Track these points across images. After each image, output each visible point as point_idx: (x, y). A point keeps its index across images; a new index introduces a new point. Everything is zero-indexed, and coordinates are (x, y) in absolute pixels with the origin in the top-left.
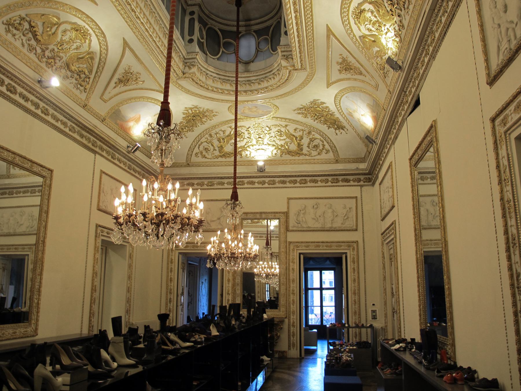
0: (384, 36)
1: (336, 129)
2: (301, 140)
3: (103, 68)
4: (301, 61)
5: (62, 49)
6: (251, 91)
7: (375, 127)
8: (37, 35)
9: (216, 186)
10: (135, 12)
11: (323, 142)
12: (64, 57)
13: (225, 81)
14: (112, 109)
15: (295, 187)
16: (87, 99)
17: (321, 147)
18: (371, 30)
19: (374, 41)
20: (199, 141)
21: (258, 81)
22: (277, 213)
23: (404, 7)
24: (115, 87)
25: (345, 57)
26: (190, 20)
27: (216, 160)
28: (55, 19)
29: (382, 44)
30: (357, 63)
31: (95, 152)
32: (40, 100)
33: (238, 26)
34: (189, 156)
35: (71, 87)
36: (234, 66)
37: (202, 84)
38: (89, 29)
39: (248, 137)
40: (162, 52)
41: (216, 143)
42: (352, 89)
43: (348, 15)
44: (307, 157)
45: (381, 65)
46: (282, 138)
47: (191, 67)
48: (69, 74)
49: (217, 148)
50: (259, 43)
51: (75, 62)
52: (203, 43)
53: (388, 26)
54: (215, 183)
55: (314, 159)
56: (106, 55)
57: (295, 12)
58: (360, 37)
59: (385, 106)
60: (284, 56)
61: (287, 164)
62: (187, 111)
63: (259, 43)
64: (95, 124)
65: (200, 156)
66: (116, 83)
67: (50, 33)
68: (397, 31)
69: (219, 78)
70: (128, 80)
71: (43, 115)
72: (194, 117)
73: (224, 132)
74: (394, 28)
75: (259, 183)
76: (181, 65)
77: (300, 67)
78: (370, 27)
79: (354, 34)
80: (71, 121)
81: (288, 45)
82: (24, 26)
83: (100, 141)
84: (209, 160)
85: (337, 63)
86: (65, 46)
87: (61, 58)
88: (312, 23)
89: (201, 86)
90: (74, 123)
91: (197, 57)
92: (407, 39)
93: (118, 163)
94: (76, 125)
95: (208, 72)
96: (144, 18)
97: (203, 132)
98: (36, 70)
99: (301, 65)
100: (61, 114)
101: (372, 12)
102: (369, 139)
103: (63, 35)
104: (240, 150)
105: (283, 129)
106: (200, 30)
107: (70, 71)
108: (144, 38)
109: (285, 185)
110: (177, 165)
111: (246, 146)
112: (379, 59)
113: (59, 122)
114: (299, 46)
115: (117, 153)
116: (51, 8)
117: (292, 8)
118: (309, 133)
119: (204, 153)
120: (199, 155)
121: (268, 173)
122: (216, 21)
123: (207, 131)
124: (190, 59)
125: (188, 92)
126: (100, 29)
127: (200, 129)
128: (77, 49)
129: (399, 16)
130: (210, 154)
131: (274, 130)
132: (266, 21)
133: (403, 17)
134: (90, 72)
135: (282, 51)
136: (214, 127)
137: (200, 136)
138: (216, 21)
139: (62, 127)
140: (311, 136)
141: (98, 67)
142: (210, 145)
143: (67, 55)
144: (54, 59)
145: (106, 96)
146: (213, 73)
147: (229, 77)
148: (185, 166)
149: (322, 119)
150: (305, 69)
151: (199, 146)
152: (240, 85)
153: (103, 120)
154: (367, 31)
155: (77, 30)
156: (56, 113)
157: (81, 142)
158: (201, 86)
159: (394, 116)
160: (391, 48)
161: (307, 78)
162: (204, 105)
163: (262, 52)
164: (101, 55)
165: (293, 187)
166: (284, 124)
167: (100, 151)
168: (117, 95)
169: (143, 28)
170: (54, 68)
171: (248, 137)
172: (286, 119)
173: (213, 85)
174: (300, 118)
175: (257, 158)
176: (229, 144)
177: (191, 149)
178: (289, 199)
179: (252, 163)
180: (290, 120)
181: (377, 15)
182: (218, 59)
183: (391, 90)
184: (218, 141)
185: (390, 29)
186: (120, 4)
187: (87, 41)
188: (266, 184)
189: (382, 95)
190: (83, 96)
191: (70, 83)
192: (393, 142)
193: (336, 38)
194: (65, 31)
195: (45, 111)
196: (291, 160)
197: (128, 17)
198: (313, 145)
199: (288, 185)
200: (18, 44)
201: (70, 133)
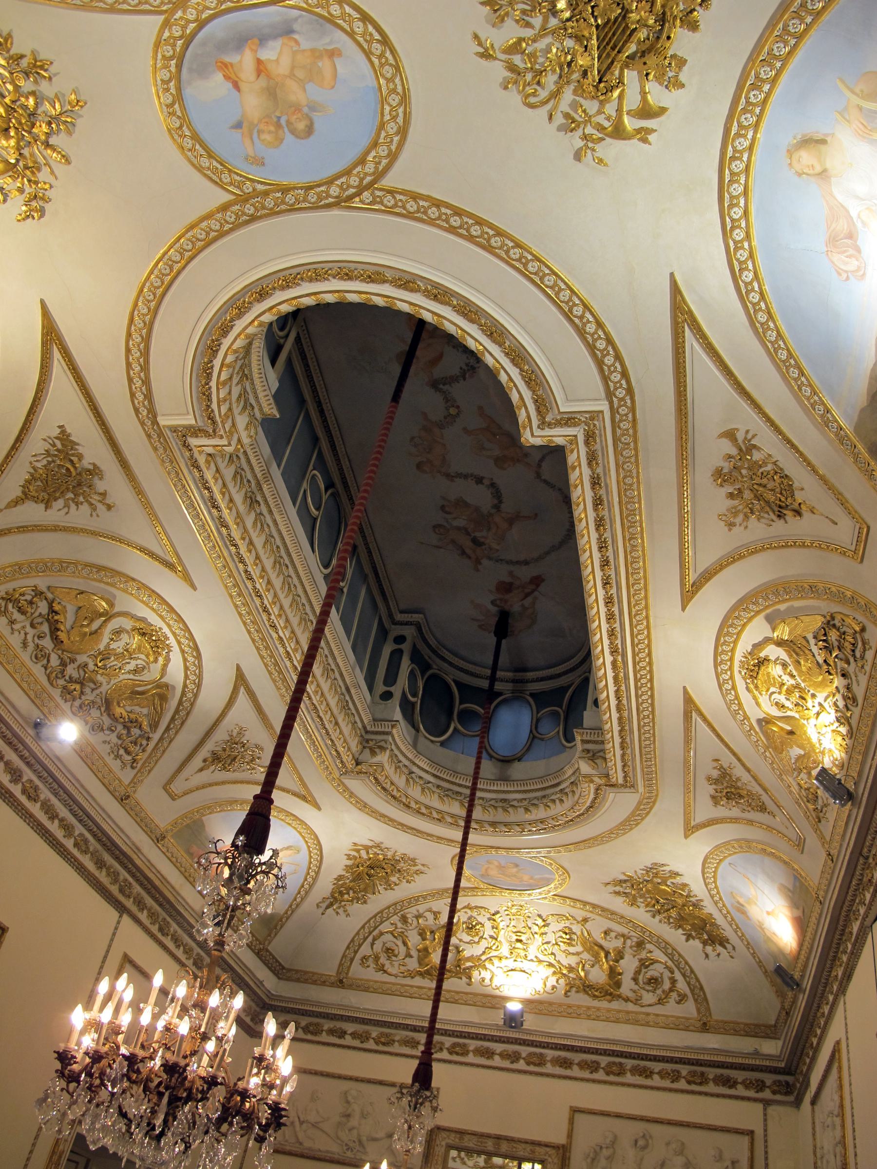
0: (813, 721)
1: (705, 943)
2: (617, 961)
3: (182, 724)
4: (624, 766)
5: (105, 667)
6: (506, 824)
7: (801, 945)
8: (58, 630)
9: (396, 1048)
10: (269, 614)
11: (672, 972)
12: (105, 683)
13: (450, 793)
14: (185, 816)
15: (594, 1081)
16: (134, 783)
17: (667, 985)
18: (783, 706)
19: (791, 733)
20: (376, 928)
21: (525, 803)
22: (539, 1144)
23: (854, 656)
24: (201, 770)
25: (725, 766)
26: (393, 653)
27: (408, 981)
28: (104, 604)
29: (809, 739)
30: (754, 783)
31: (121, 909)
32: (28, 764)
33: (493, 679)
34: (347, 959)
35: (104, 750)
36: (473, 760)
37: (395, 793)
38: (170, 635)
39: (492, 937)
40: (316, 708)
41: (414, 939)
42: (745, 846)
43: (731, 668)
44: (631, 1007)
45: (808, 789)
46: (572, 949)
47: (377, 750)
48: (107, 721)
49: (414, 953)
50: (538, 720)
51: (126, 699)
52: (413, 705)
53: (820, 697)
54: (397, 1038)
55: (648, 1014)
56: (196, 696)
57: (612, 653)
58: (759, 721)
59: (821, 893)
60: (588, 751)
61: (578, 1016)
62: (358, 851)
63: (538, 720)
64: (138, 844)
65: (373, 965)
66: (205, 761)
67: (87, 630)
68: (840, 711)
69: (438, 787)
70: (235, 758)
71: (23, 799)
72: (370, 871)
74: (835, 704)
75: (504, 1055)
76: (354, 744)
77: (621, 781)
78: (782, 698)
79: (744, 712)
80: (84, 826)
81: (599, 729)
82: (37, 607)
83: (141, 885)
84: (392, 979)
85: (709, 779)
86: (112, 662)
87: (97, 685)
88: (651, 680)
89: (393, 796)
90: (90, 831)
91: (394, 731)
92: (866, 730)
93: (171, 945)
94: (94, 836)
95: (415, 769)
96: (286, 627)
97: (388, 907)
98: (37, 701)
99: (625, 777)
100: (65, 805)
101: (784, 665)
102: (782, 975)
103: (112, 639)
104: (469, 964)
105: (576, 928)
106: (412, 675)
107: (109, 715)
108: (280, 672)
109: (568, 1072)
110: (315, 977)
111: (483, 958)
112: (803, 776)
113: (56, 821)
114: (621, 731)
115: (175, 920)
116: (101, 581)
117: (606, 642)
118: (640, 945)
119: (383, 960)
120: (371, 962)
121: (529, 1032)
122: (451, 664)
123: (398, 908)
124: (377, 733)
125: (364, 807)
126: (192, 638)
127: (382, 898)
128: (135, 671)
129: (843, 675)
130: (396, 964)
131: (556, 926)
132: (559, 676)
133: (854, 678)
134: (154, 726)
135: (584, 742)
136: (415, 900)
137: (380, 916)
138: (451, 664)
139: (59, 834)
140: (643, 955)
141: (173, 719)
142: (400, 943)
143: (112, 682)
144: (82, 684)
145: (178, 786)
146: (427, 772)
147: (460, 785)
148: (332, 985)
149: (673, 913)
150: (632, 786)
151: (374, 939)
152: (484, 808)
153: (159, 839)
154: (774, 707)
155: (144, 634)
156: (54, 801)
157: (95, 878)
158: (393, 796)
159: (842, 918)
160: (830, 750)
161: (637, 808)
162: (399, 843)
163: (542, 740)
164: (183, 693)
165: (587, 1080)
166: (580, 914)
167: (134, 909)
168: (204, 787)
169: (281, 650)
170: (77, 703)
171: (492, 937)
172: (585, 903)
173: (422, 799)
174: (619, 905)
175: (506, 992)
177: (354, 945)
178: (575, 1111)
179: (494, 1001)
180: (594, 906)
181: (795, 673)
182: (442, 744)
183: (834, 852)
184: (420, 934)
185: (826, 705)
186: (240, 594)
187: (161, 660)
188: (522, 1062)
189: (813, 865)
190: (127, 776)
191: (105, 742)
192: (843, 990)
193: (705, 720)
194: (118, 632)
195: (31, 791)
196: (589, 1008)
197: (254, 622)
198: (648, 976)
199: (576, 1072)
200: (15, 640)
201: (75, 852)
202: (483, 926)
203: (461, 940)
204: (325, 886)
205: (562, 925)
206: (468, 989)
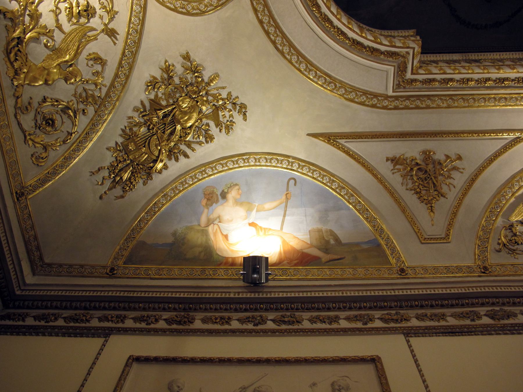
105: (95, 22)
166: (121, 25)
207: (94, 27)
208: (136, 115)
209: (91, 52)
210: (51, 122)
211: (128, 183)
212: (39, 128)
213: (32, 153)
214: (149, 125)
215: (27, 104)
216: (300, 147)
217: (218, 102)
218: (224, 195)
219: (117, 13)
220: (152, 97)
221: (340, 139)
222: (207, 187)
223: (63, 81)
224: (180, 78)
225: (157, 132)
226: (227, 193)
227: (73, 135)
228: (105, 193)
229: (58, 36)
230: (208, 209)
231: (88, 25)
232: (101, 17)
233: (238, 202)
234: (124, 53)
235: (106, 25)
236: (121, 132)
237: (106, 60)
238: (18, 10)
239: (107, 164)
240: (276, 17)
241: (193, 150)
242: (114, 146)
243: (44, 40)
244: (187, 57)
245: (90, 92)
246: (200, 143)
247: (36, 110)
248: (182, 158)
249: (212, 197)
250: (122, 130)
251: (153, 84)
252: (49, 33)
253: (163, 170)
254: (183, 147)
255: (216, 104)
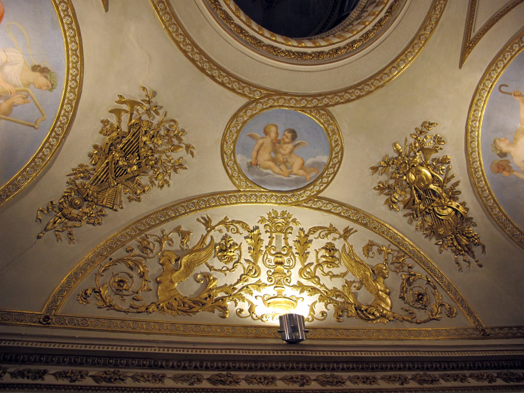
46: (335, 271)
73: (184, 235)
84: (122, 315)
105: (339, 244)
111: (239, 286)
131: (317, 244)
176: (191, 278)
202: (240, 249)
203: (211, 268)
204: (57, 182)
205: (323, 242)
206: (222, 322)
207: (342, 246)
208: (415, 223)
209: (362, 253)
210: (421, 296)
211: (471, 240)
212: (426, 306)
213: (446, 316)
214: (426, 212)
215: (407, 313)
216: (471, 76)
217: (416, 147)
218: (503, 155)
219: (331, 225)
220: (401, 206)
221: (470, 37)
222: (491, 168)
223: (386, 280)
224: (391, 178)
225: (432, 206)
226: (501, 151)
227: (429, 280)
228: (476, 262)
229: (350, 277)
230: (513, 171)
231: (340, 252)
232: (335, 239)
233: (513, 142)
234: (365, 225)
235: (341, 237)
236: (427, 239)
237: (369, 240)
238: (334, 305)
239: (453, 256)
240: (356, 83)
241: (453, 176)
242: (439, 246)
243: (353, 289)
244: (375, 169)
245: (394, 259)
246: (448, 169)
247: (411, 306)
248: (457, 188)
249: (502, 166)
250: (426, 237)
251: (391, 203)
252: (349, 284)
253: (466, 206)
254: (448, 185)
255: (418, 149)
